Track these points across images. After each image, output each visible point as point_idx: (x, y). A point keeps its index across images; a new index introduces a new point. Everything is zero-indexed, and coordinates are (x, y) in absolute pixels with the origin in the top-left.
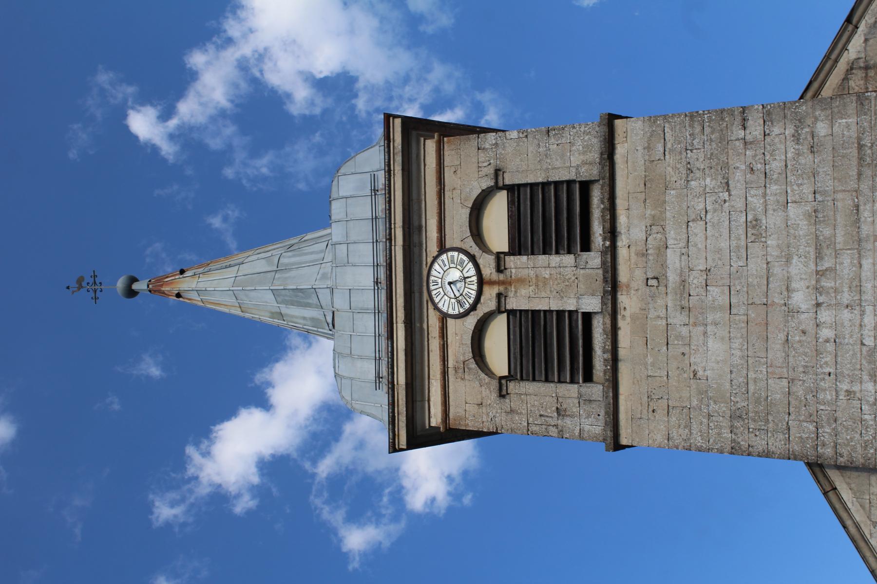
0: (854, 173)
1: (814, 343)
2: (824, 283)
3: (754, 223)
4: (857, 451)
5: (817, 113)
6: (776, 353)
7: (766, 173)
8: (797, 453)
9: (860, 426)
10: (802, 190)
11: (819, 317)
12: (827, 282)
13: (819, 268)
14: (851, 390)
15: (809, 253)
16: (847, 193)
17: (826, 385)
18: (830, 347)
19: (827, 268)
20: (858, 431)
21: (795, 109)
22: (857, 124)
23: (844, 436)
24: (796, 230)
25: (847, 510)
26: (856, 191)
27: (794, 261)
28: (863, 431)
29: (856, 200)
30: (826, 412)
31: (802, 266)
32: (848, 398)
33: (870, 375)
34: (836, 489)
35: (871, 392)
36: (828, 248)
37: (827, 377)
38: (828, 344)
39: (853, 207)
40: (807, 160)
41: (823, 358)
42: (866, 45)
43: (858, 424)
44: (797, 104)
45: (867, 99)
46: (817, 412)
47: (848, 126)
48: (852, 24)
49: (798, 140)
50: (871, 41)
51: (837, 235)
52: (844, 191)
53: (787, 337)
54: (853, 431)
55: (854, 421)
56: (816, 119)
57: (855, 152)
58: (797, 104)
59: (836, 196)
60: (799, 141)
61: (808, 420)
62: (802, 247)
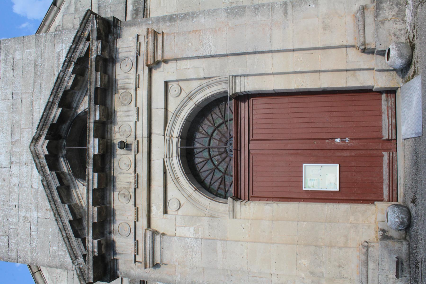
0: (32, 82)
1: (9, 186)
2: (15, 149)
4: (28, 255)
5: (16, 46)
9: (30, 239)
10: (7, 92)
11: (11, 170)
12: (16, 149)
14: (26, 216)
15: (8, 130)
16: (28, 94)
17: (14, 213)
18: (16, 189)
19: (16, 140)
20: (29, 242)
21: (6, 44)
22: (35, 52)
24: (2, 117)
26: (32, 93)
28: (31, 242)
29: (32, 98)
31: (4, 139)
32: (24, 221)
33: (35, 207)
34: (40, 270)
35: (35, 217)
36: (17, 128)
37: (14, 208)
38: (15, 187)
39: (30, 103)
40: (10, 74)
41: (12, 196)
42: (63, 18)
43: (29, 238)
44: (7, 41)
45: (40, 37)
46: (9, 230)
47: (30, 54)
48: (56, 6)
49: (6, 62)
50: (65, 16)
51: (22, 120)
52: (27, 93)
54: (26, 242)
55: (27, 235)
56: (15, 49)
57: (33, 69)
58: (7, 41)
59: (23, 96)
60: (6, 63)
61: (4, 235)
62: (5, 127)
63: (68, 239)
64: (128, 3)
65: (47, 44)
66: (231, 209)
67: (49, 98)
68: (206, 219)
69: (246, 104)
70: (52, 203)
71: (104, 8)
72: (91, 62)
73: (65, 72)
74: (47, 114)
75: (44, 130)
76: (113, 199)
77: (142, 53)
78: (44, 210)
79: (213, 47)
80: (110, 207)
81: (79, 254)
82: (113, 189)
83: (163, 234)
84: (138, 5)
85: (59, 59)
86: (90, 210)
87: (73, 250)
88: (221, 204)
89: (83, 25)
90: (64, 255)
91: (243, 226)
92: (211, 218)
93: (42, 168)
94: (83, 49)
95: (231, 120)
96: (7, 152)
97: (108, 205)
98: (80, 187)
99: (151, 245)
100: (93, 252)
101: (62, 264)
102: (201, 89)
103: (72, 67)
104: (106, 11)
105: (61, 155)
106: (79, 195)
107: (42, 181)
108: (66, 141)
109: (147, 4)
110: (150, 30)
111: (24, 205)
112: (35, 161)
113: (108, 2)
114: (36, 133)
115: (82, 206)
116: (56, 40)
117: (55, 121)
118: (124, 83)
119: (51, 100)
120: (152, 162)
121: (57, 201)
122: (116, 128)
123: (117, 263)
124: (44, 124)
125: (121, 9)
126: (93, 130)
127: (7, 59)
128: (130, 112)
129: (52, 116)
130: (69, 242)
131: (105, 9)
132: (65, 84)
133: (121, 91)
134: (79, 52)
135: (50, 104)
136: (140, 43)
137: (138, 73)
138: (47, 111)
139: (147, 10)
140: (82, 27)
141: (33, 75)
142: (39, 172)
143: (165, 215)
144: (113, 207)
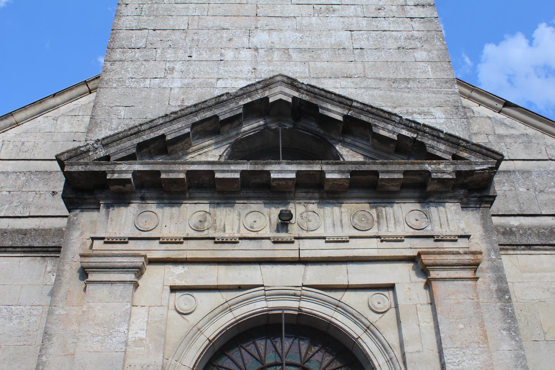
0: (382, 75)
1: (221, 46)
3: (331, 9)
5: (434, 52)
6: (210, 22)
7: (377, 18)
8: (117, 35)
11: (245, 50)
13: (290, 51)
14: (174, 71)
15: (305, 44)
17: (180, 54)
18: (216, 57)
21: (437, 38)
23: (130, 67)
24: (326, 36)
25: (71, 100)
27: (297, 34)
30: (154, 54)
31: (292, 39)
32: (167, 69)
33: (188, 84)
34: (90, 93)
35: (172, 85)
38: (219, 55)
39: (349, 74)
40: (392, 44)
41: (206, 52)
44: (441, 39)
45: (452, 85)
47: (424, 72)
48: (503, 107)
49: (409, 39)
50: (489, 121)
51: (322, 63)
53: (227, 29)
54: (135, 72)
56: (429, 51)
60: (408, 39)
61: (148, 42)
62: (310, 39)
63: (135, 134)
64: (522, 217)
65: (442, 95)
67: (358, 102)
70: (193, 109)
71: (509, 180)
72: (418, 164)
73: (399, 123)
74: (332, 100)
75: (308, 95)
76: (198, 202)
77: (439, 244)
78: (182, 97)
79: (460, 367)
80: (185, 199)
81: (112, 150)
82: (214, 203)
83: (136, 285)
84: (520, 234)
85: (420, 114)
86: (181, 166)
87: (117, 140)
89: (478, 149)
90: (112, 128)
93: (248, 93)
94: (440, 150)
96: (272, 43)
97: (187, 195)
98: (217, 151)
99: (119, 265)
100: (113, 172)
101: (97, 124)
102: (384, 348)
103: (408, 134)
104: (504, 183)
105: (268, 120)
106: (206, 150)
107: (227, 93)
108: (291, 128)
109: (523, 249)
110: (479, 257)
111: (191, 68)
112: (259, 82)
113: (519, 185)
114: (303, 83)
115: (188, 154)
116: (449, 108)
117: (322, 111)
118: (388, 217)
119: (355, 104)
120: (258, 267)
121: (196, 116)
122: (313, 207)
123: (93, 209)
124: (316, 94)
125: (511, 207)
126: (308, 169)
127: (414, 40)
128: (340, 228)
129: (329, 106)
130: (131, 135)
131: (507, 182)
132: (382, 125)
133: (374, 212)
134: (434, 143)
135: (349, 103)
136: (456, 241)
137: (406, 239)
138: (337, 99)
139: (514, 250)
140: (474, 147)
141: (392, 77)
142: (241, 89)
143: (169, 288)
144: (184, 202)
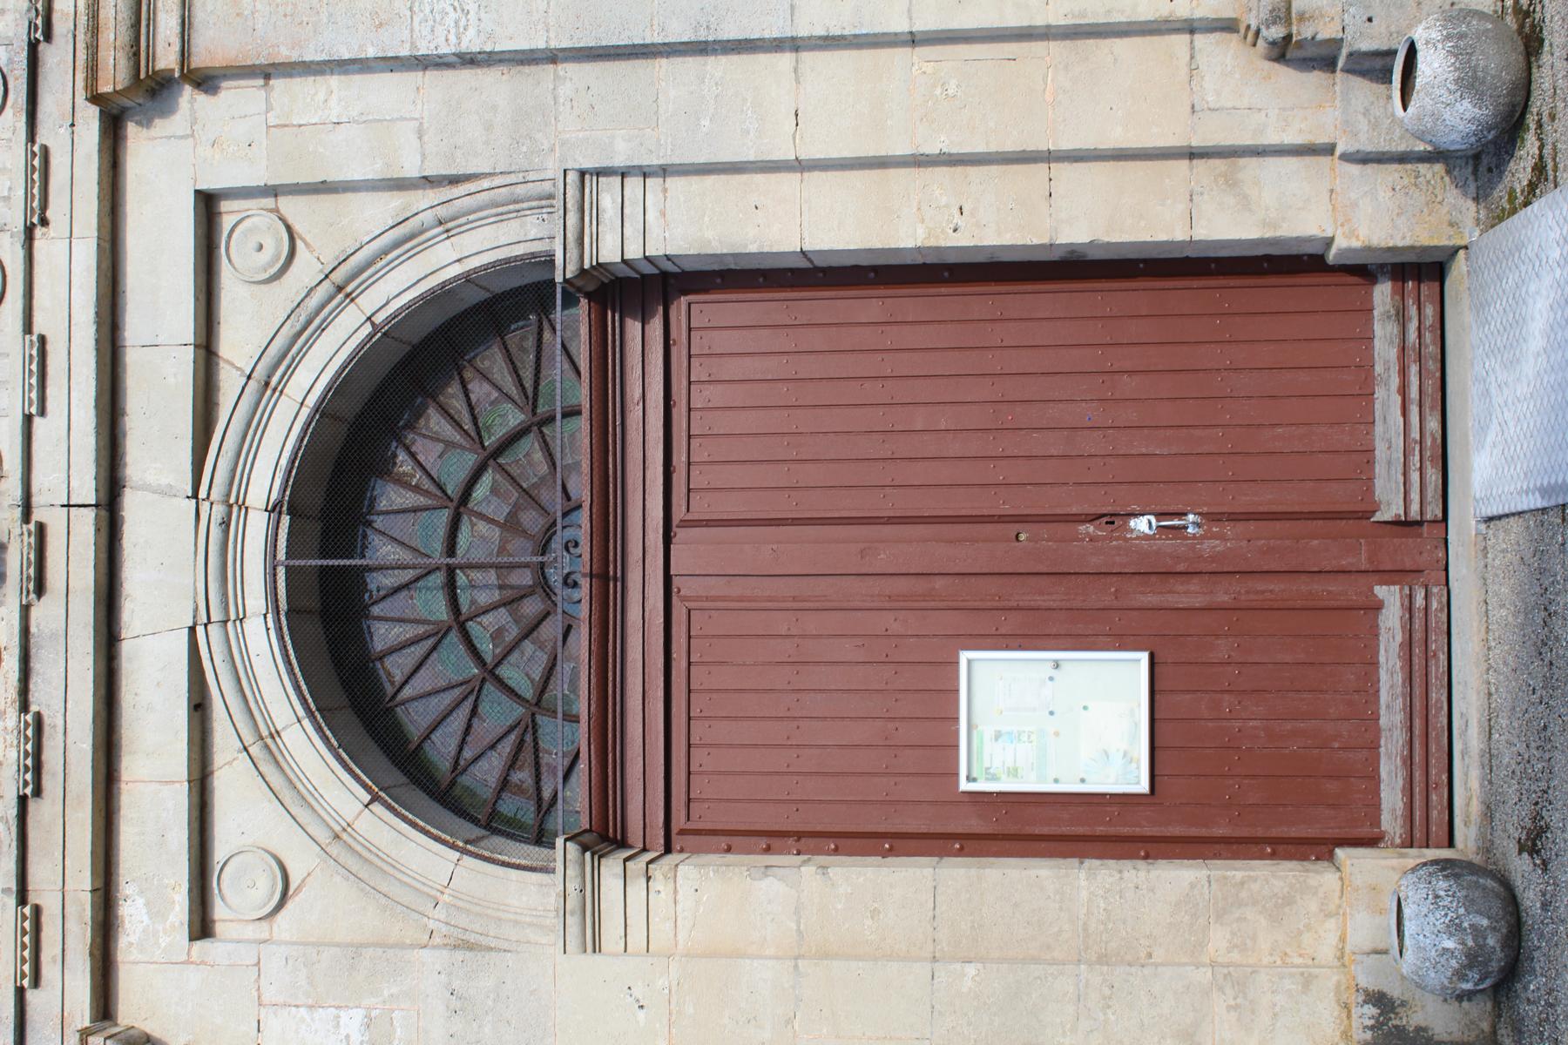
66: (573, 901)
68: (434, 959)
69: (656, 325)
77: (61, 26)
88: (514, 873)
91: (637, 992)
92: (459, 955)
95: (571, 413)
102: (406, 241)
120: (126, 648)
137: (40, 140)
143: (198, 944)
